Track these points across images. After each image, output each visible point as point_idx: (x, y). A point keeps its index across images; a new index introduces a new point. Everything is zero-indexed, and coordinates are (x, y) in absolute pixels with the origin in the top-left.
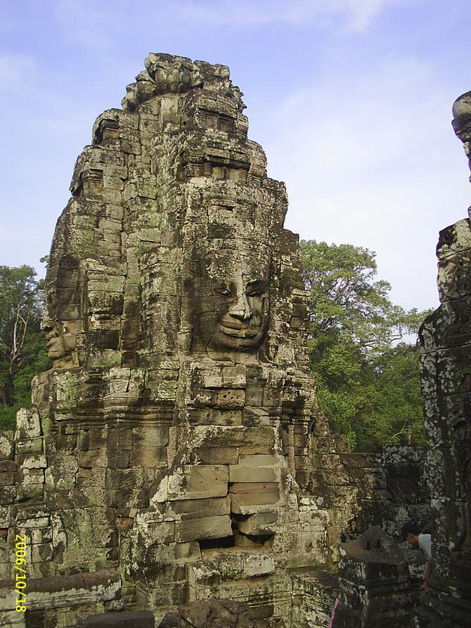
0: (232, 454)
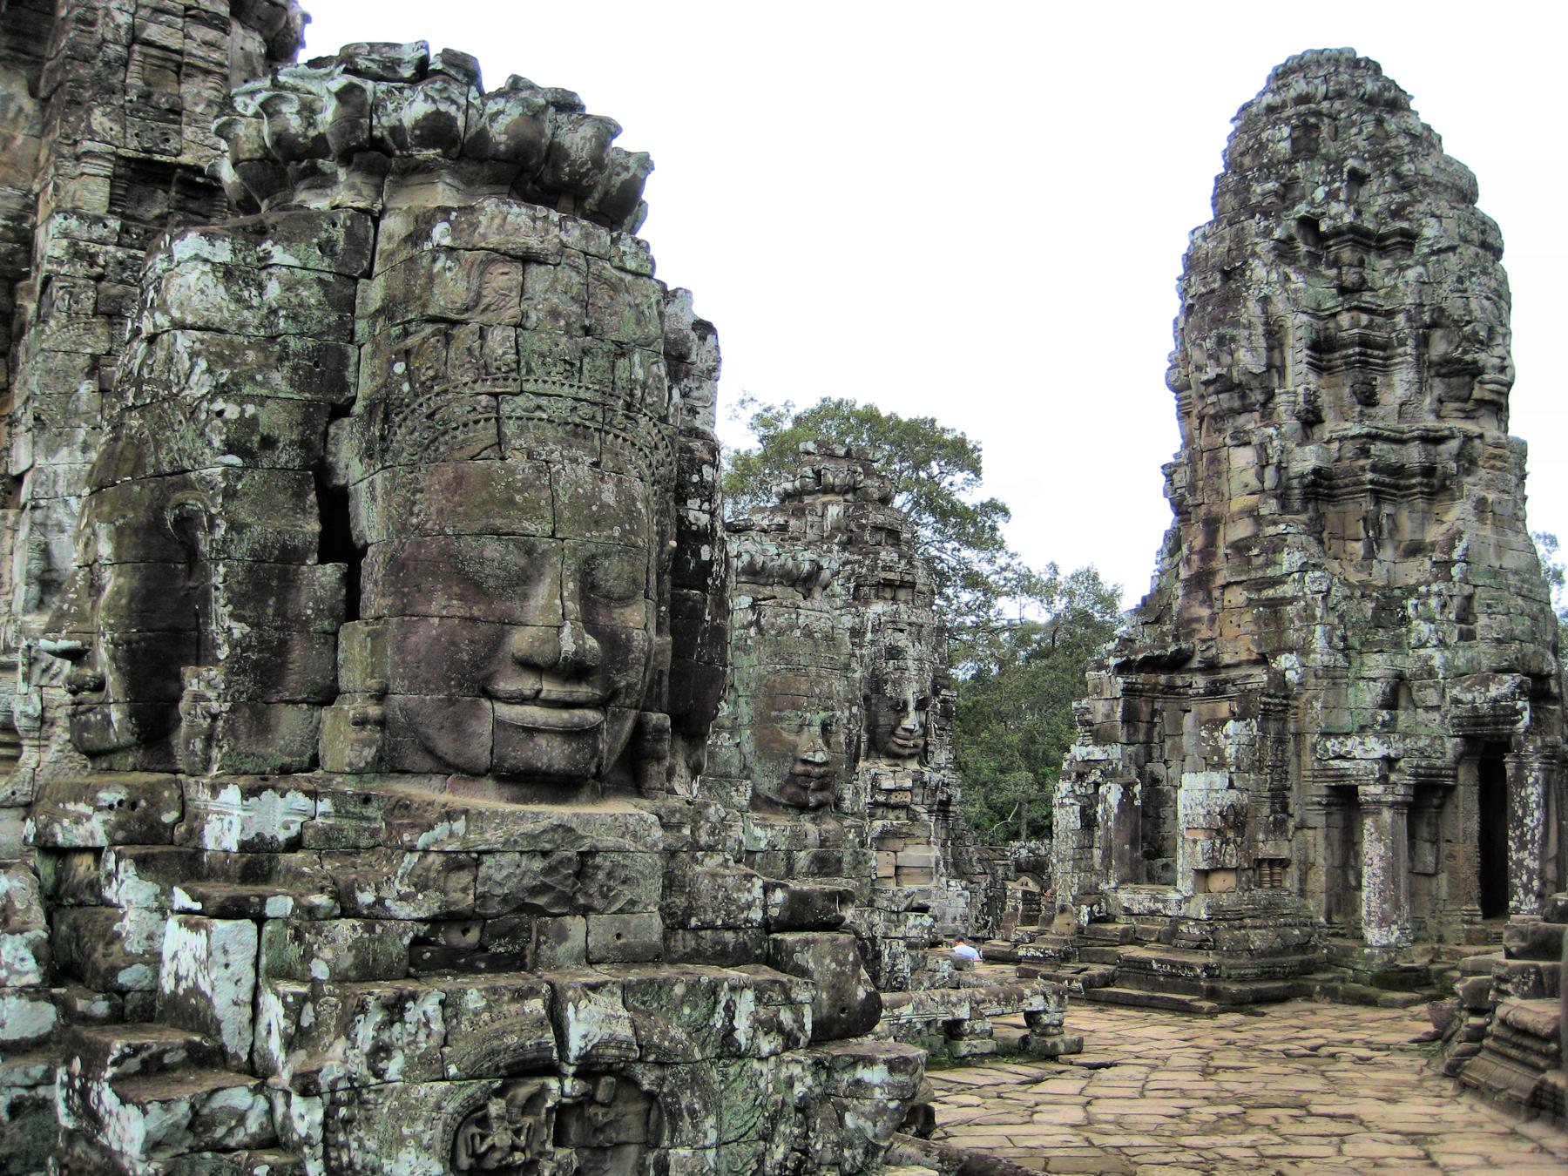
0: (899, 844)
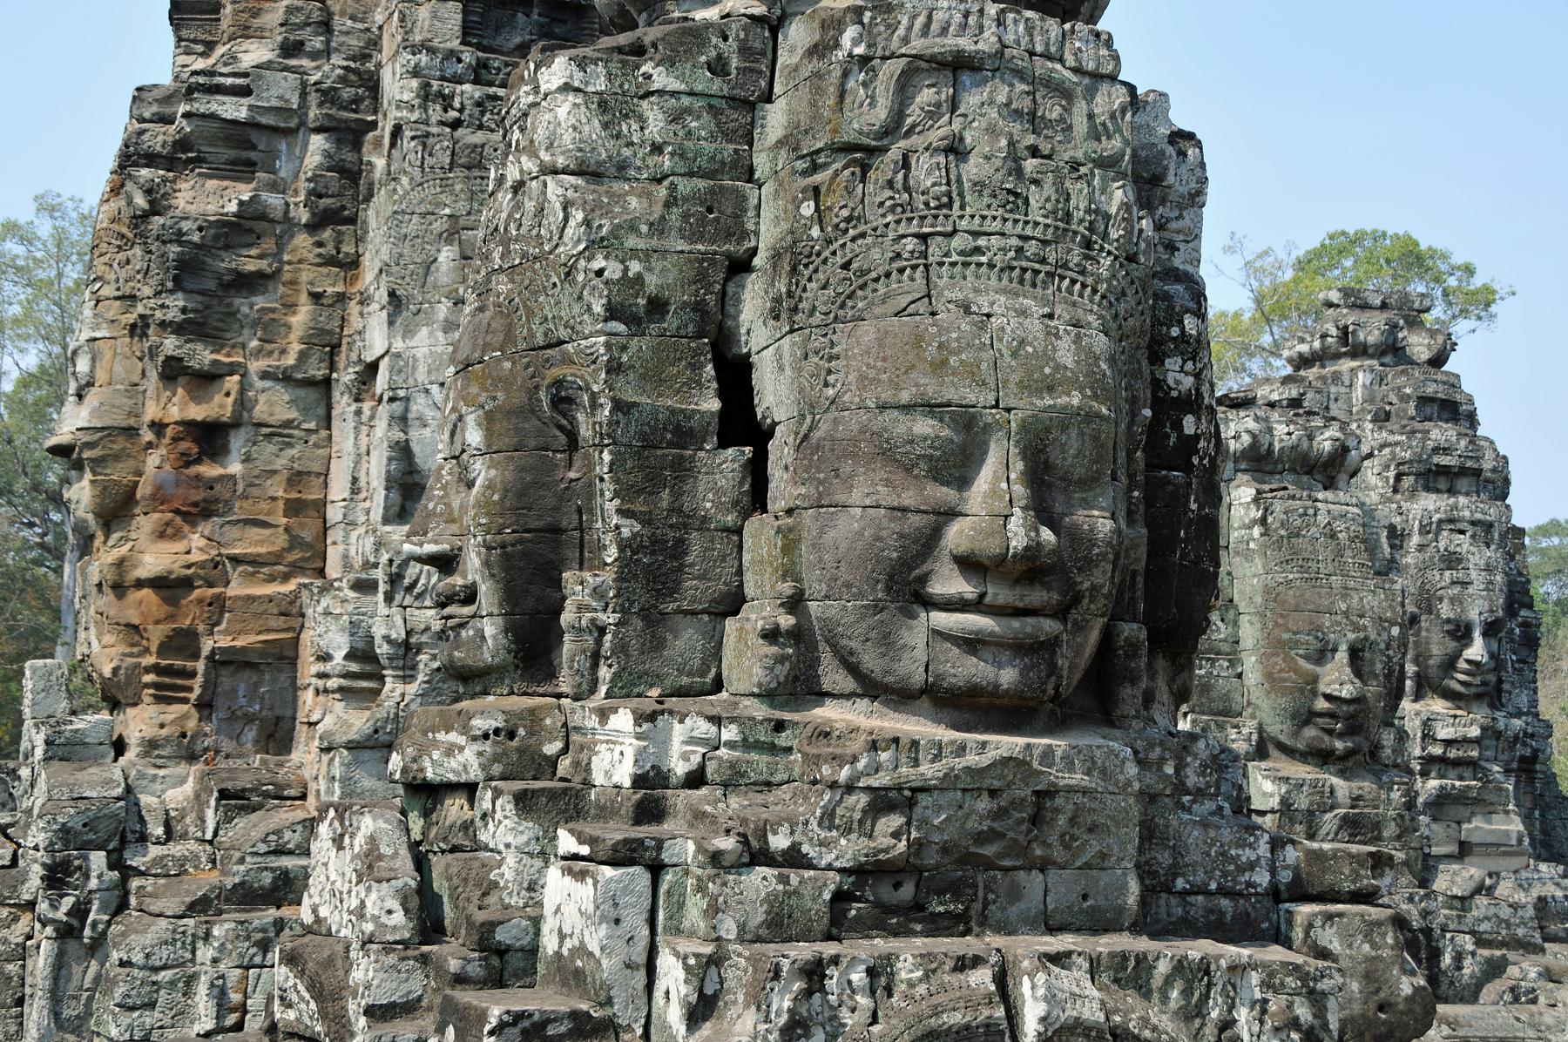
0: (1463, 812)
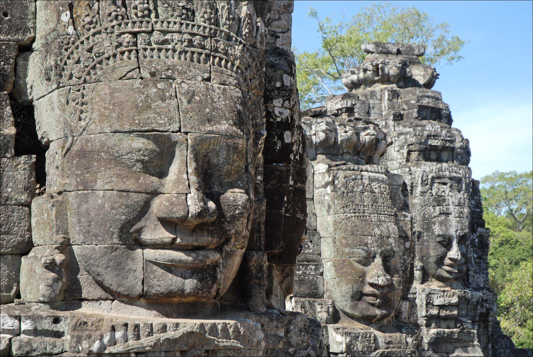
0: (450, 347)
